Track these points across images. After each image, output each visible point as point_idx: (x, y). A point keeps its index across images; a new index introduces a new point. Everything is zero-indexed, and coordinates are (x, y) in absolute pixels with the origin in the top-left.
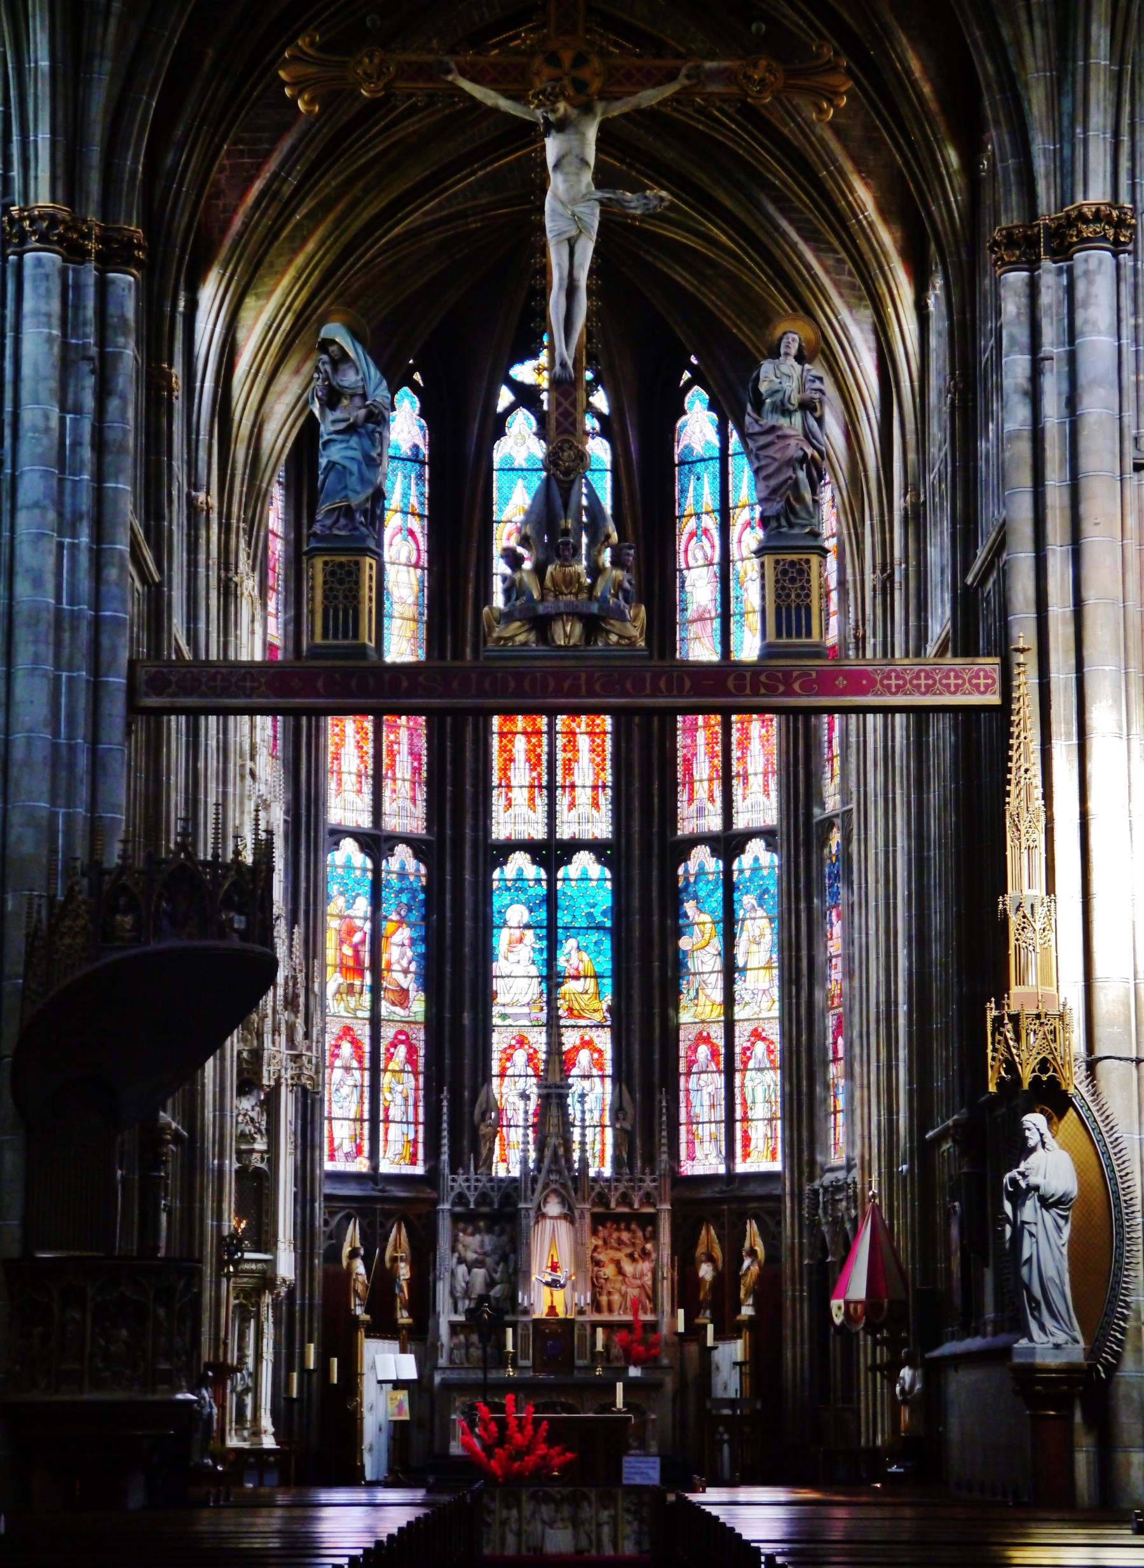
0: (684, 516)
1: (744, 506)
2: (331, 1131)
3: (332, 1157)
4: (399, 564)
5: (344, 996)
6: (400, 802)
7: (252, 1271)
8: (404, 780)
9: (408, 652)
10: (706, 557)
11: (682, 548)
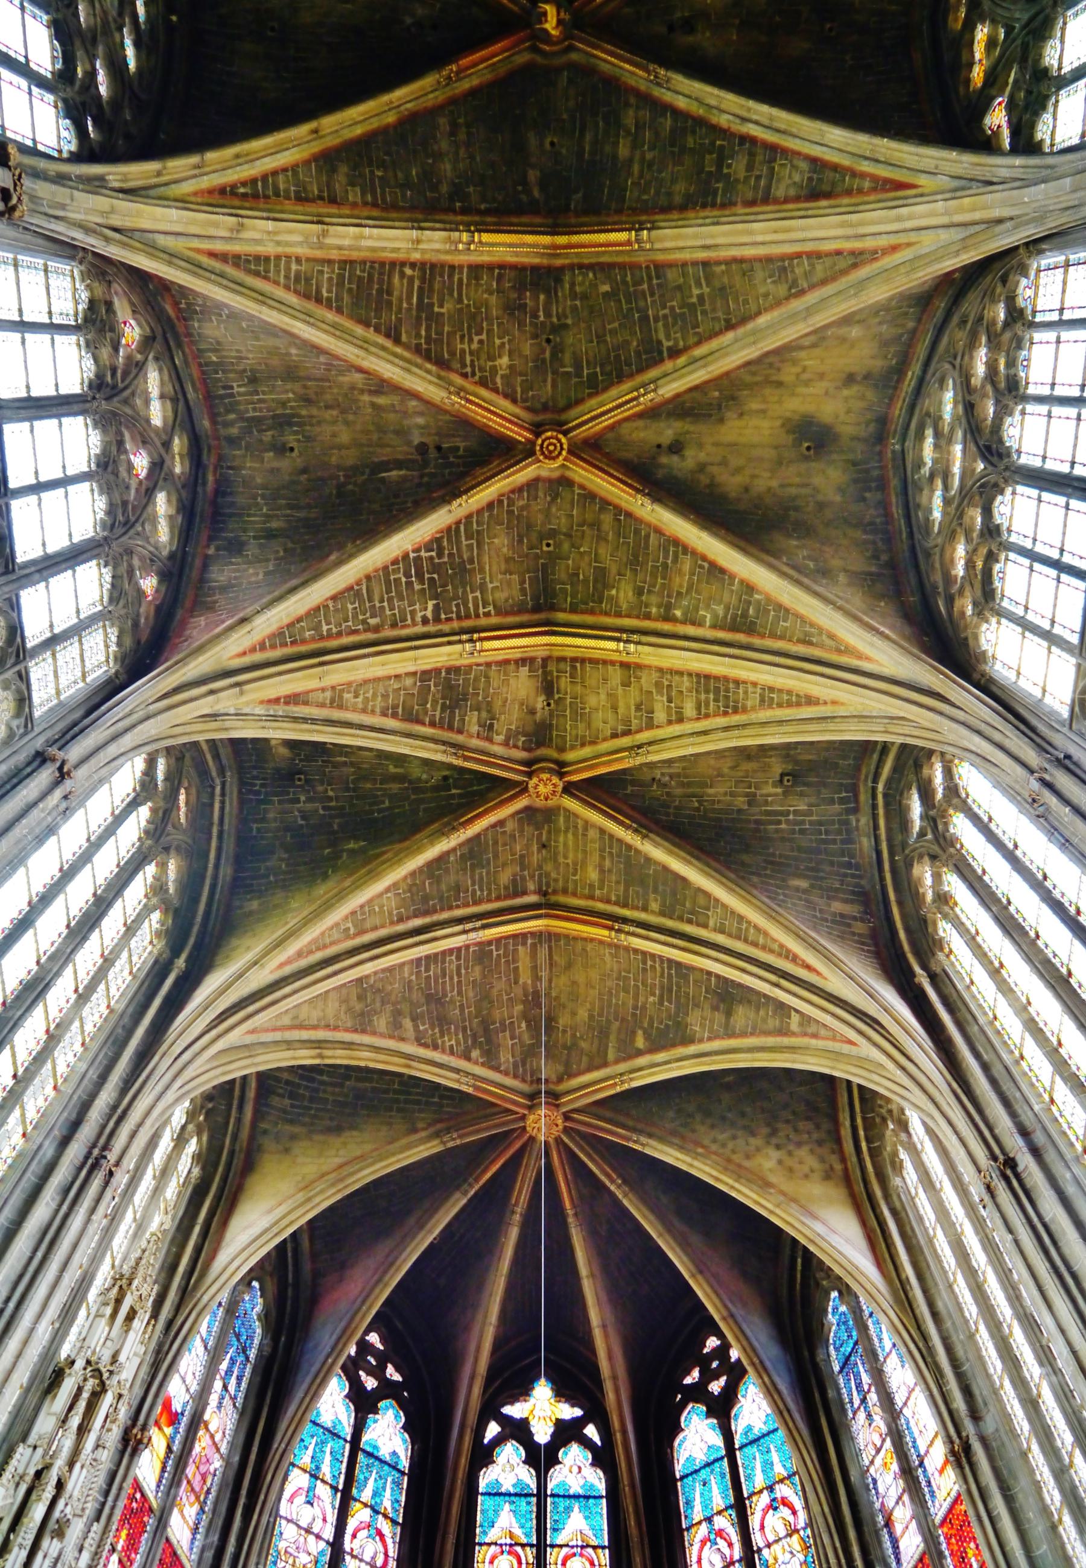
0: (693, 1525)
1: (761, 1492)
4: (361, 1560)
10: (723, 1557)
11: (695, 1559)
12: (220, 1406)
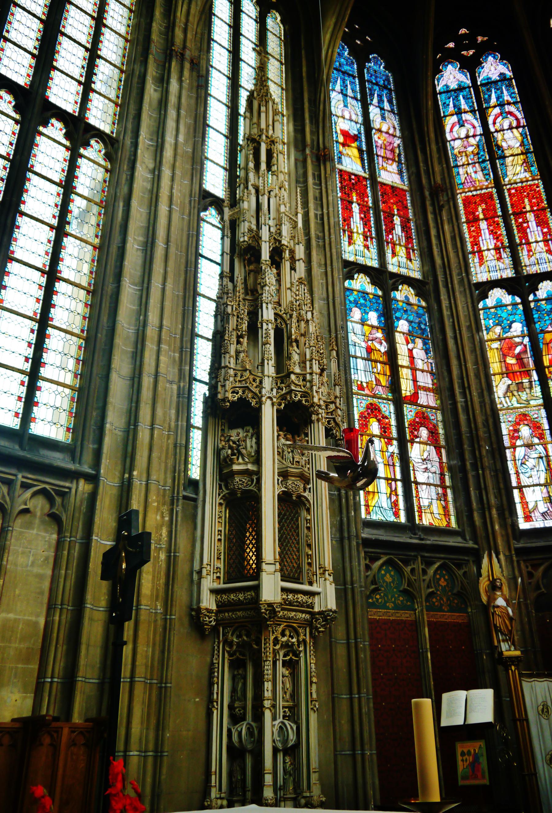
2: (522, 497)
3: (528, 518)
5: (515, 393)
6: (538, 256)
7: (239, 603)
8: (537, 242)
9: (523, 171)
12: (383, 118)
